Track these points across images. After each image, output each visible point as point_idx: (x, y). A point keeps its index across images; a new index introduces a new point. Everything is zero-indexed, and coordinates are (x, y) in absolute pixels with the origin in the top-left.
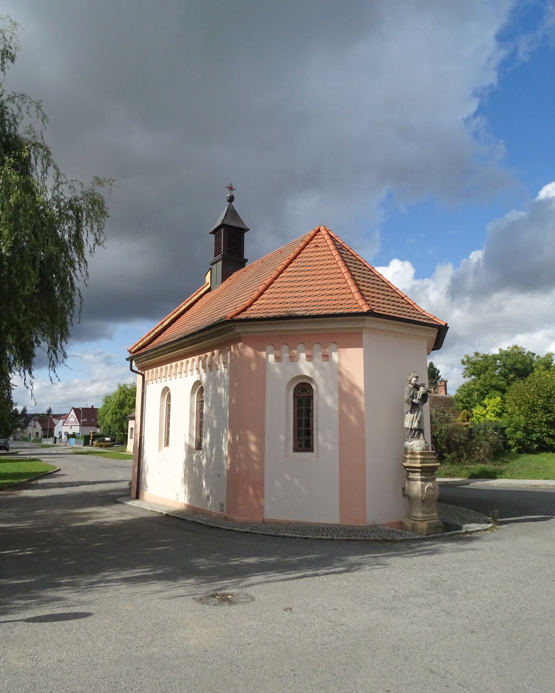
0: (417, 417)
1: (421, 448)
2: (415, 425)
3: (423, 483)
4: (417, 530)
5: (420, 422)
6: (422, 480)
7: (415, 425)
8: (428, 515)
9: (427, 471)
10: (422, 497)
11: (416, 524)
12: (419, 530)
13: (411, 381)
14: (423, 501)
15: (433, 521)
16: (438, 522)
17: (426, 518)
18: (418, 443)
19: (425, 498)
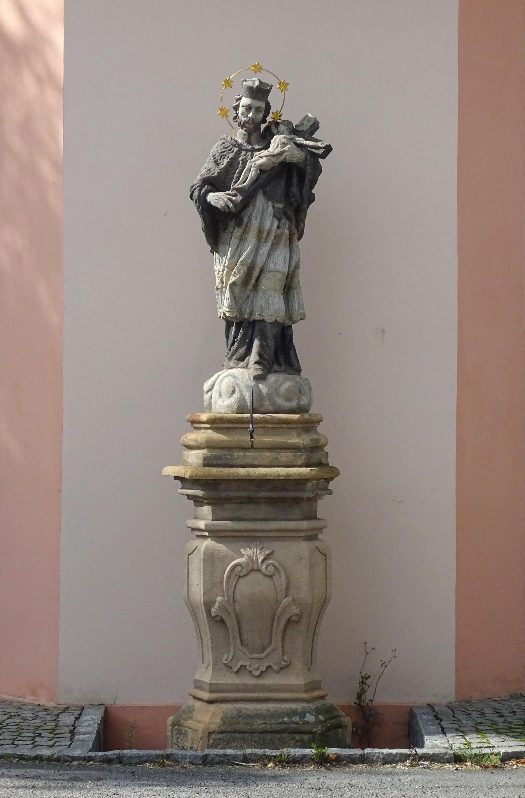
1: (232, 401)
3: (221, 547)
4: (185, 734)
6: (215, 534)
8: (252, 681)
9: (251, 500)
10: (208, 605)
11: (191, 710)
12: (190, 735)
13: (236, 108)
14: (218, 622)
15: (271, 706)
16: (294, 713)
17: (236, 689)
18: (226, 380)
19: (222, 607)
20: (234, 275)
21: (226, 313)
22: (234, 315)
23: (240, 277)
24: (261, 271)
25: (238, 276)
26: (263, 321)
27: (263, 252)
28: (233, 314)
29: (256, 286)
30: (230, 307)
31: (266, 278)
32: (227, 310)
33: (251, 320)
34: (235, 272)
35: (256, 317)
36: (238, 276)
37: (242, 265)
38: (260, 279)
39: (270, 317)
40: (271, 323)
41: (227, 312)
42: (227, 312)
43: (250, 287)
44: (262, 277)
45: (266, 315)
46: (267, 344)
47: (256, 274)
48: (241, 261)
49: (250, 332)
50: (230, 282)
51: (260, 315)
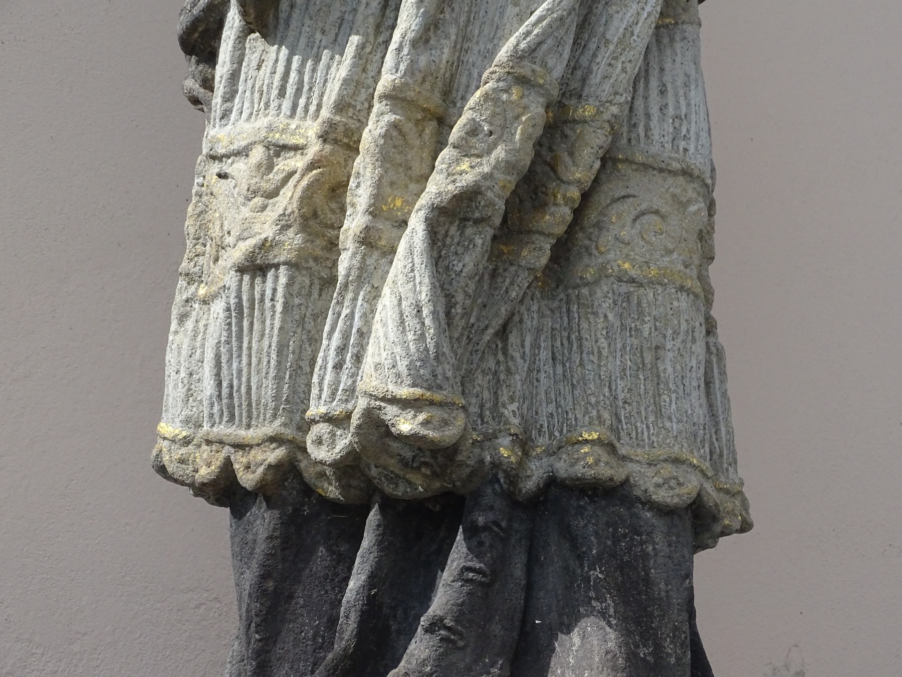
0: (429, 114)
2: (383, 346)
5: (524, 247)
7: (383, 346)
20: (464, 149)
21: (390, 412)
22: (450, 434)
23: (508, 166)
24: (608, 160)
25: (499, 152)
26: (609, 493)
27: (629, 31)
28: (445, 423)
29: (564, 250)
30: (426, 371)
31: (627, 209)
32: (404, 392)
33: (529, 485)
34: (473, 130)
35: (587, 462)
36: (499, 152)
37: (522, 81)
38: (593, 215)
39: (668, 470)
40: (666, 512)
41: (404, 404)
42: (404, 404)
43: (537, 255)
44: (602, 198)
45: (640, 453)
46: (658, 648)
47: (579, 169)
48: (518, 57)
49: (518, 570)
50: (438, 187)
51: (611, 448)
